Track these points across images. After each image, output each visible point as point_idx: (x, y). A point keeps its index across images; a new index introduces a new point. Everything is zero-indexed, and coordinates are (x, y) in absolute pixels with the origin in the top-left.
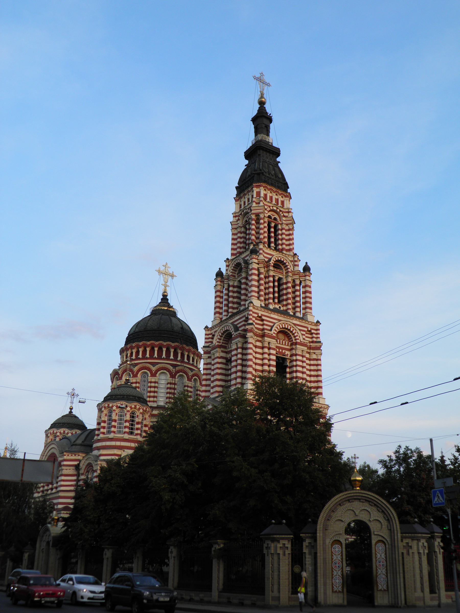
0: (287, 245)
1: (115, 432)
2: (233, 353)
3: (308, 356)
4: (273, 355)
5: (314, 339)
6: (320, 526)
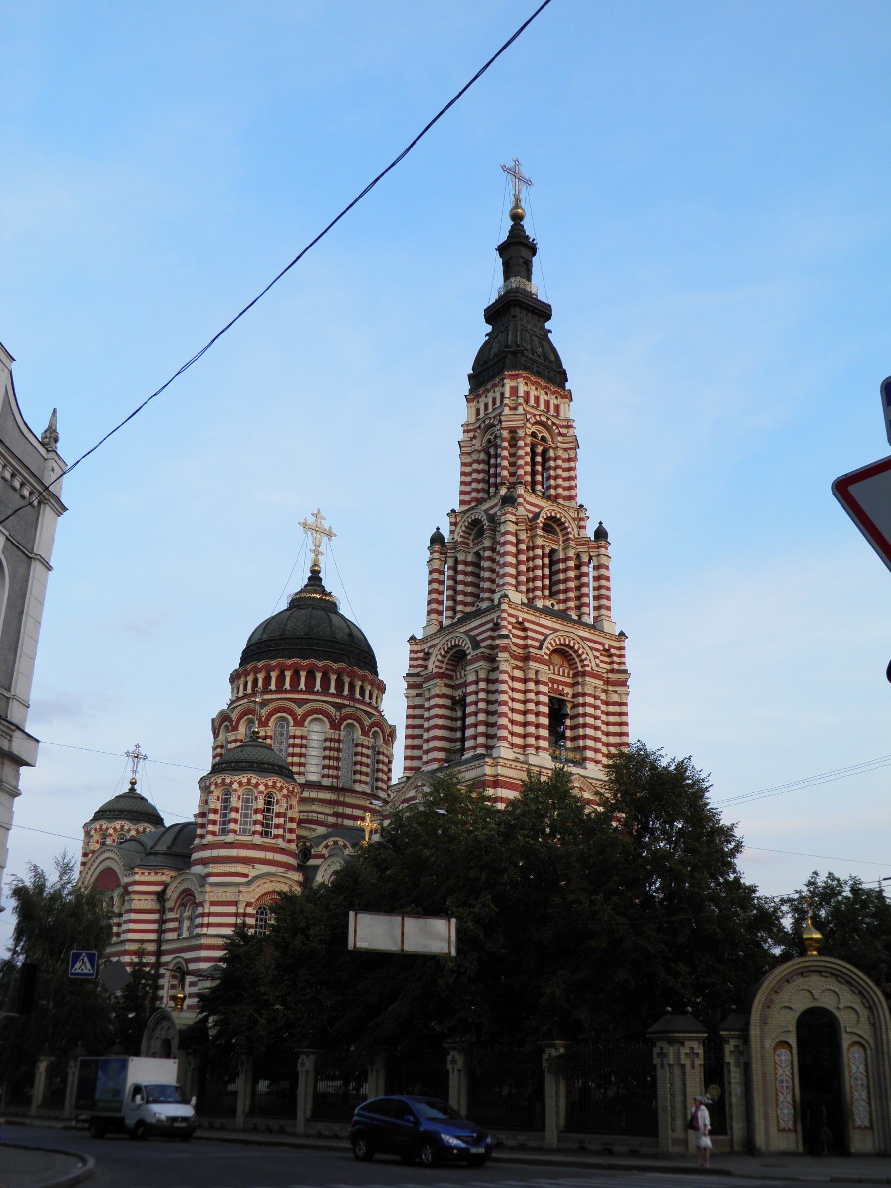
0: (565, 489)
1: (237, 831)
2: (471, 688)
3: (603, 696)
4: (544, 694)
5: (616, 667)
6: (755, 1018)
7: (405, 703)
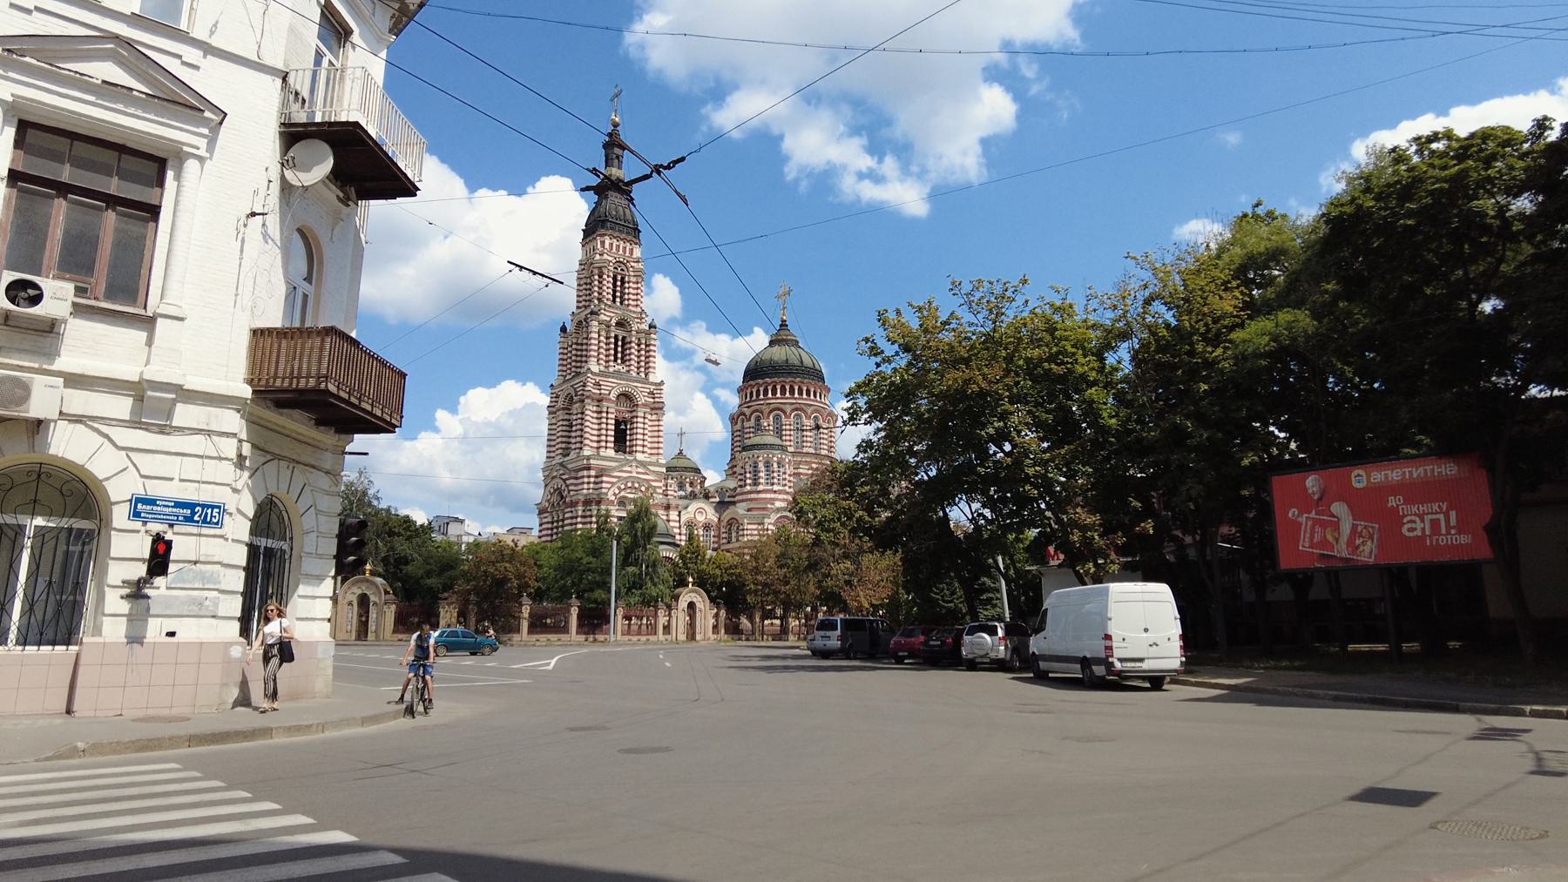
5: (657, 400)
7: (547, 422)
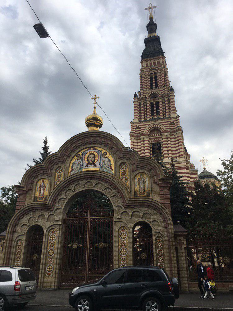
3: (173, 137)
5: (176, 126)
